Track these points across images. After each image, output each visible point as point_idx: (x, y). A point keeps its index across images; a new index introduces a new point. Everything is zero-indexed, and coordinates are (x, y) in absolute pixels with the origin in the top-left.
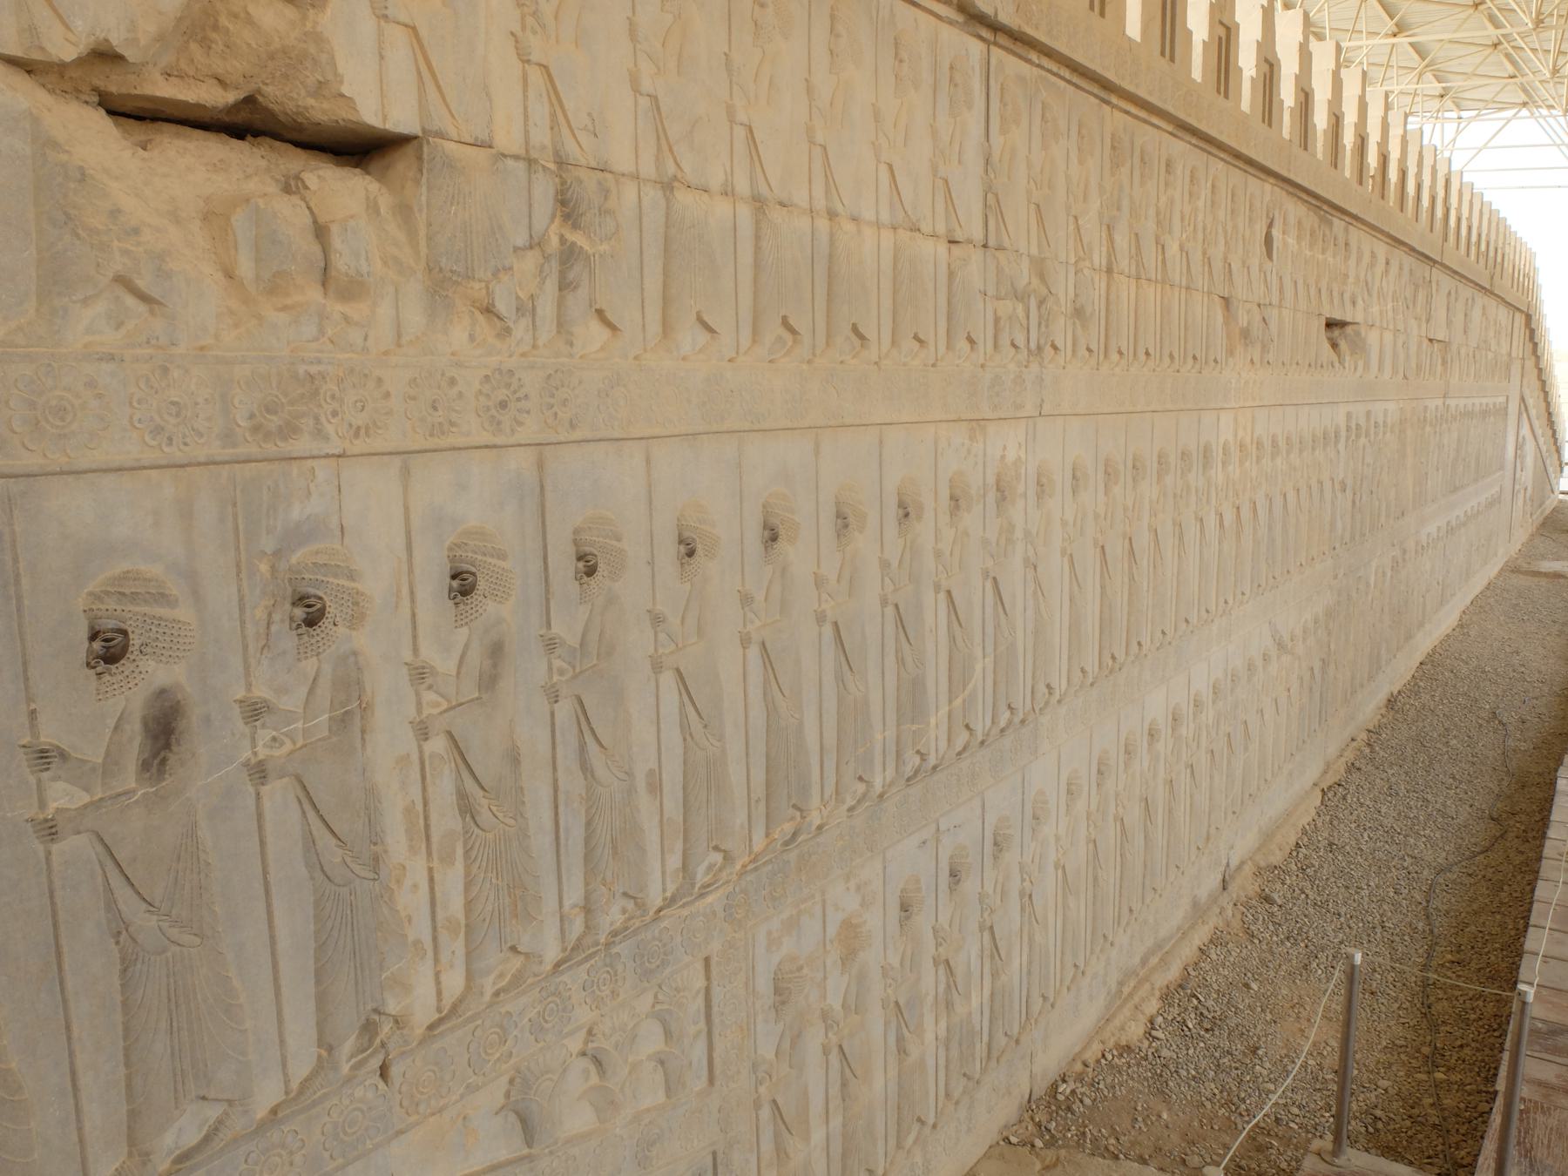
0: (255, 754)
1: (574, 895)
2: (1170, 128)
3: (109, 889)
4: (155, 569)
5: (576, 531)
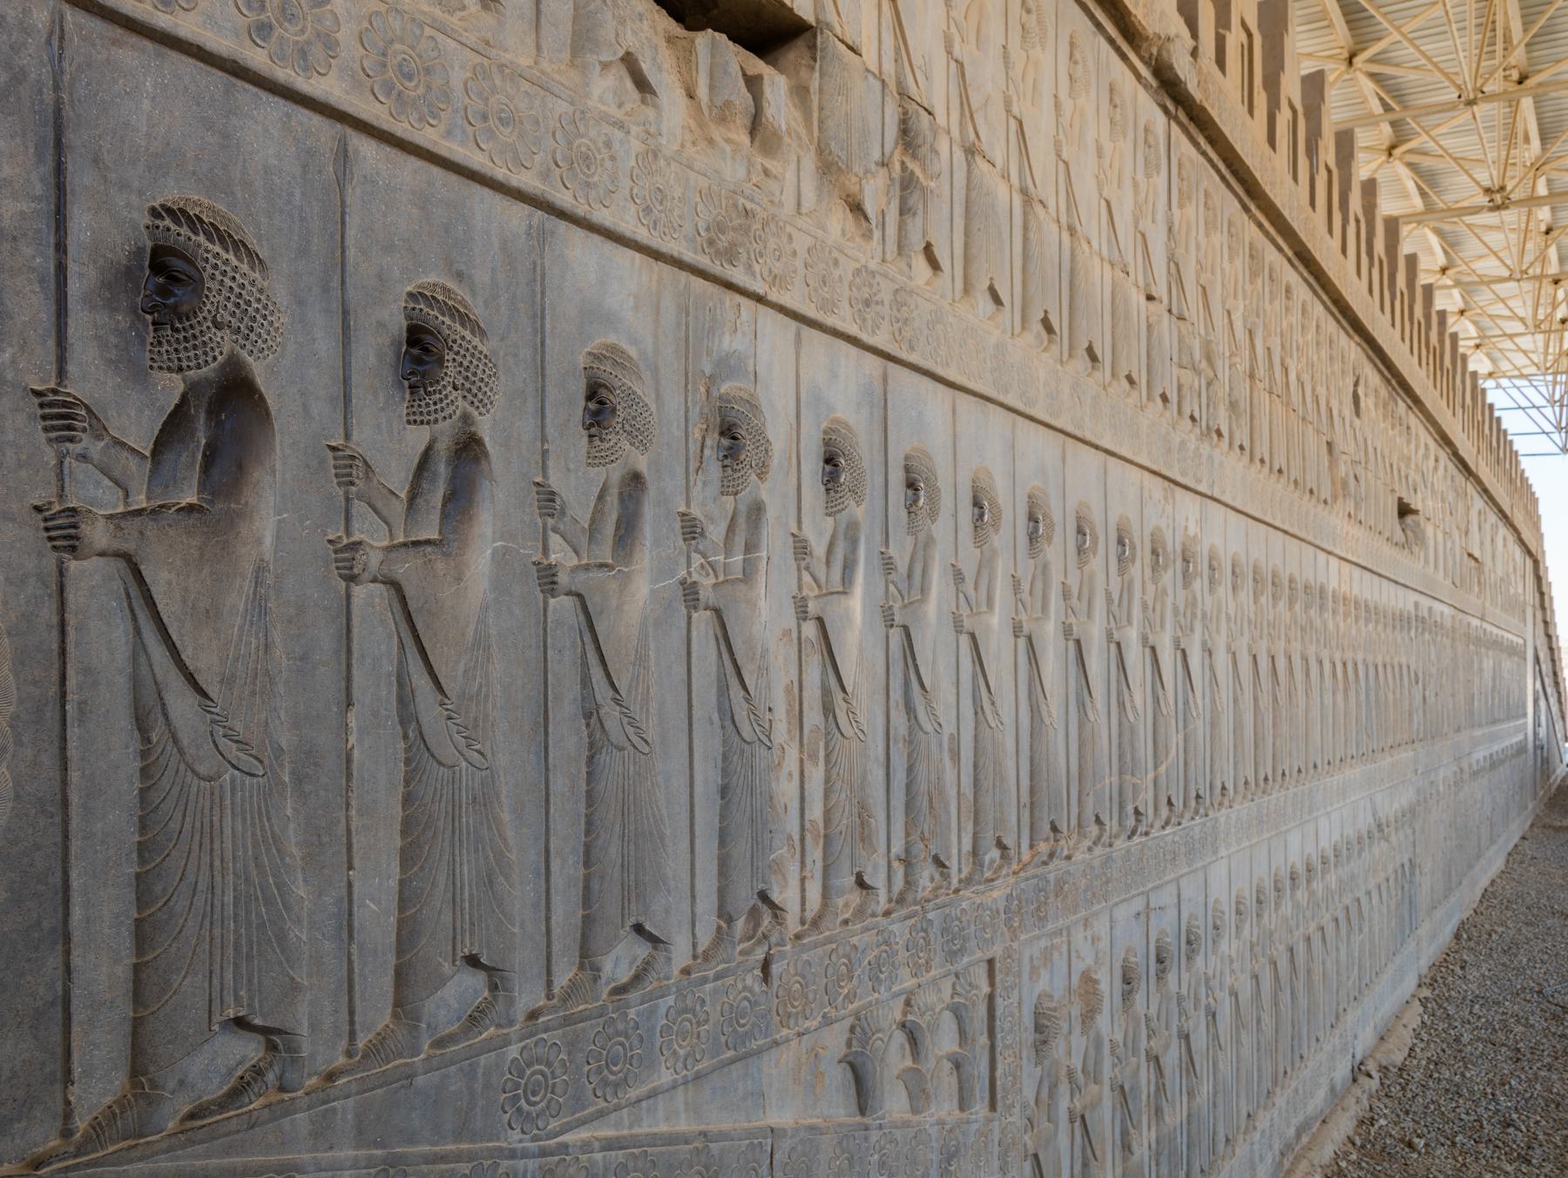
0: (689, 573)
1: (898, 847)
2: (1290, 253)
3: (585, 664)
4: (633, 352)
5: (907, 458)
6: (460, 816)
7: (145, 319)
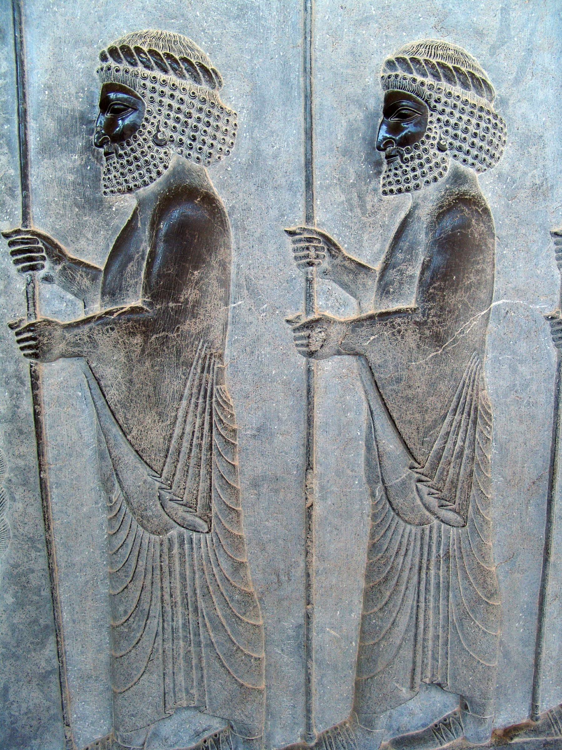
6: (428, 568)
7: (98, 153)
